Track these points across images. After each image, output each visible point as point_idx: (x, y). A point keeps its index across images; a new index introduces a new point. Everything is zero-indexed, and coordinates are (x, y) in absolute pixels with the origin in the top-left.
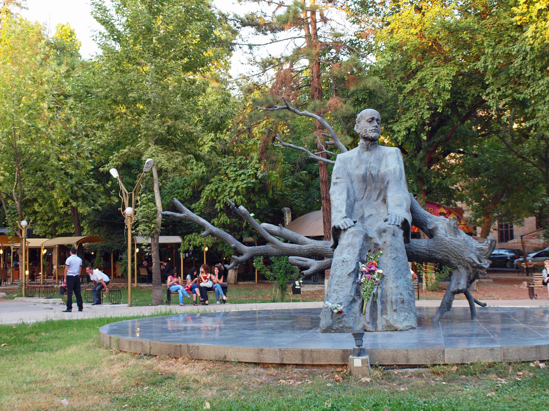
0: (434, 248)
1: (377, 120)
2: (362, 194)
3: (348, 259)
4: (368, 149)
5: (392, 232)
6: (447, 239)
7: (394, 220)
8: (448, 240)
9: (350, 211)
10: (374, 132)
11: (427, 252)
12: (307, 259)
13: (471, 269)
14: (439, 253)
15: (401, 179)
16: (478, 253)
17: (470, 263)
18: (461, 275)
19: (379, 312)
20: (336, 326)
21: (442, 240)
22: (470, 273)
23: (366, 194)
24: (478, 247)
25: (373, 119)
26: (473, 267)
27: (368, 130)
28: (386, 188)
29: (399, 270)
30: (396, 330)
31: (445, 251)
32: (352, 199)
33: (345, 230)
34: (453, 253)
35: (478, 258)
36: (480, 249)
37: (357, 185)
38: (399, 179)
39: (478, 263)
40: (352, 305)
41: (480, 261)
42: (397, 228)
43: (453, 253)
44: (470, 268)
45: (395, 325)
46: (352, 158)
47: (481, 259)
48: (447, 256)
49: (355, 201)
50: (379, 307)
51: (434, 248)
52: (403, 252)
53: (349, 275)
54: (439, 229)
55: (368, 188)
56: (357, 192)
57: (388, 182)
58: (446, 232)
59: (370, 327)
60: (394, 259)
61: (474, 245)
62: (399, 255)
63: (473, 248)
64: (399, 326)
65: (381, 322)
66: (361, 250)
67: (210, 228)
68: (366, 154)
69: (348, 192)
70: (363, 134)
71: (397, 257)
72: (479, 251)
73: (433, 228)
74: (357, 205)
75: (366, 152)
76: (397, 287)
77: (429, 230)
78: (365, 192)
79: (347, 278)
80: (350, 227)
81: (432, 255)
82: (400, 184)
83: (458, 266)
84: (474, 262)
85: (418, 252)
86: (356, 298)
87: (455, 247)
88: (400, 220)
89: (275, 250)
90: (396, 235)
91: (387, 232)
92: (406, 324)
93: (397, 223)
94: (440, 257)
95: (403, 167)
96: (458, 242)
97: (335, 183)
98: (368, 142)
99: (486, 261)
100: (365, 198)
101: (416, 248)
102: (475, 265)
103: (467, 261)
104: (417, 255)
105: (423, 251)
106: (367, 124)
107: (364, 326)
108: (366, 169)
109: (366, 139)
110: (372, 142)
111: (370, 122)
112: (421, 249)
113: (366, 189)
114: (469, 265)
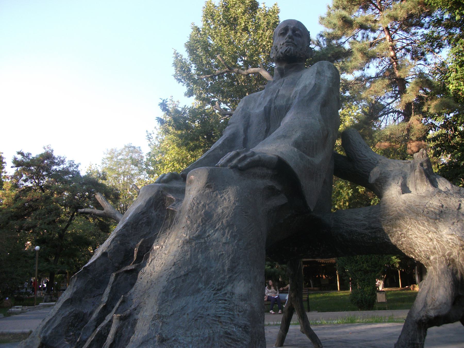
11: (367, 232)
38: (307, 98)
98: (283, 66)
108: (270, 101)
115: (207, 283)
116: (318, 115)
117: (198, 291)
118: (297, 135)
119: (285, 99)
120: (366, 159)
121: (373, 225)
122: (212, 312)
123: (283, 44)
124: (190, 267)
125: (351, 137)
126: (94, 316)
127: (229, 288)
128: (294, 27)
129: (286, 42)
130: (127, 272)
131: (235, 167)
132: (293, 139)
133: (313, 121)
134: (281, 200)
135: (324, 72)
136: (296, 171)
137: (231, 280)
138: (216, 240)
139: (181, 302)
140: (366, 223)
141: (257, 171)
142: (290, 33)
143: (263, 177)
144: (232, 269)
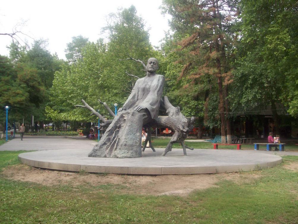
1: (154, 63)
6: (171, 117)
15: (156, 89)
17: (179, 129)
19: (114, 150)
20: (93, 154)
25: (151, 62)
29: (131, 131)
30: (118, 158)
32: (136, 99)
39: (181, 129)
40: (104, 146)
42: (137, 112)
45: (117, 156)
46: (142, 81)
49: (138, 100)
50: (115, 147)
55: (145, 94)
56: (139, 95)
59: (108, 156)
60: (129, 126)
64: (119, 156)
65: (113, 154)
72: (184, 123)
76: (125, 139)
78: (143, 96)
86: (107, 143)
88: (141, 108)
91: (130, 114)
92: (124, 155)
93: (137, 110)
95: (159, 85)
105: (163, 123)
107: (106, 155)
111: (150, 64)
113: (144, 94)
115: (132, 133)
116: (156, 95)
117: (131, 134)
118: (151, 102)
122: (133, 138)
126: (112, 138)
130: (117, 131)
131: (137, 111)
132: (150, 103)
134: (146, 117)
136: (150, 111)
137: (137, 133)
139: (129, 136)
141: (142, 111)
142: (152, 64)
144: (137, 131)
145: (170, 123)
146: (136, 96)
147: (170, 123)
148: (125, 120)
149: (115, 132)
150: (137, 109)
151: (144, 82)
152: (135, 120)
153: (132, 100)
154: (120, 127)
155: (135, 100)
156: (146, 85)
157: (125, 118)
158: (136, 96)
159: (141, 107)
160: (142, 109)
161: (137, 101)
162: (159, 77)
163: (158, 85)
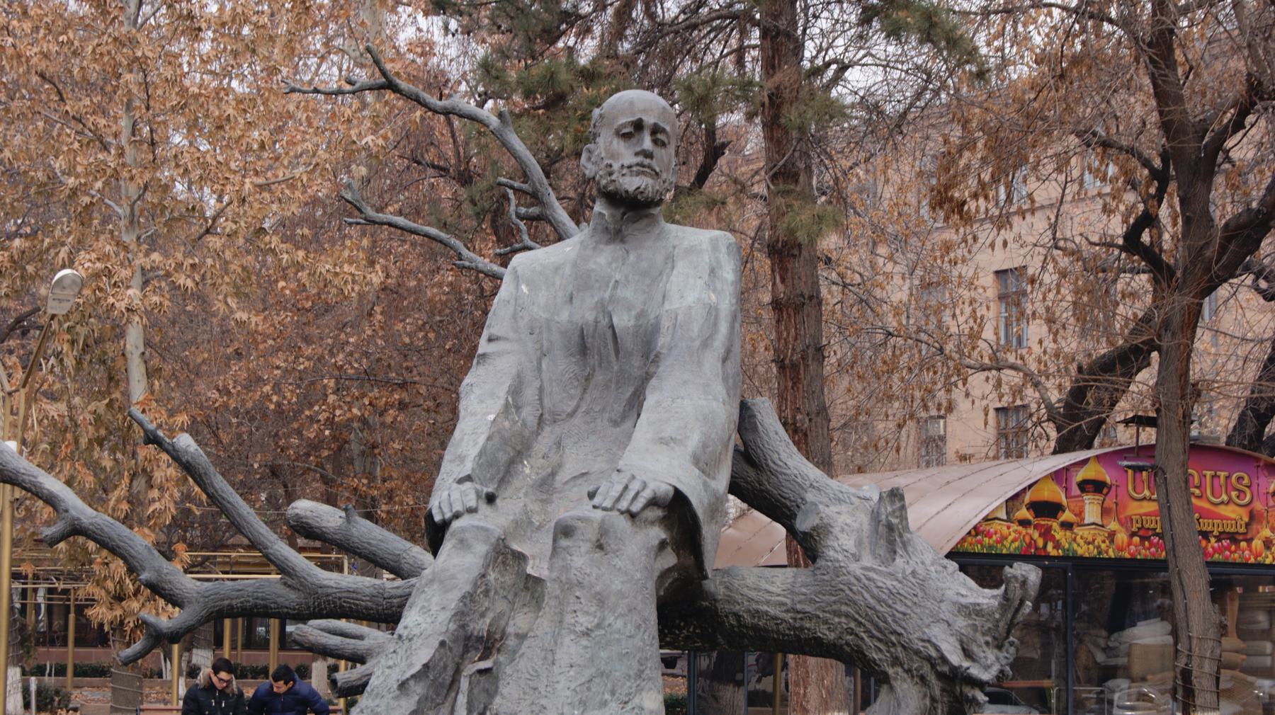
0: (812, 601)
1: (656, 130)
2: (572, 397)
3: (416, 631)
4: (616, 235)
5: (592, 534)
6: (854, 567)
7: (615, 493)
8: (859, 572)
9: (503, 457)
10: (638, 174)
11: (787, 616)
12: (362, 628)
13: (936, 686)
14: (826, 622)
15: (706, 344)
16: (961, 623)
17: (928, 659)
18: (899, 705)
21: (838, 571)
22: (933, 700)
23: (588, 397)
24: (963, 601)
25: (638, 125)
26: (941, 676)
27: (616, 166)
28: (647, 377)
31: (847, 616)
33: (445, 525)
34: (871, 621)
35: (961, 642)
36: (972, 611)
37: (561, 366)
38: (697, 343)
39: (956, 658)
41: (968, 654)
42: (623, 523)
43: (871, 621)
44: (932, 678)
46: (557, 269)
47: (975, 649)
48: (851, 632)
51: (812, 601)
52: (631, 610)
53: (403, 686)
54: (836, 531)
55: (599, 377)
57: (657, 356)
58: (859, 544)
60: (587, 633)
61: (950, 594)
62: (611, 619)
63: (943, 606)
66: (469, 598)
67: (73, 513)
68: (605, 258)
69: (516, 390)
70: (604, 182)
71: (598, 626)
73: (814, 529)
74: (544, 442)
75: (611, 247)
77: (805, 533)
78: (585, 390)
79: (396, 698)
80: (457, 516)
81: (802, 629)
82: (700, 363)
83: (891, 671)
84: (944, 659)
85: (757, 614)
87: (879, 601)
88: (647, 495)
89: (293, 596)
90: (611, 543)
93: (624, 505)
94: (832, 636)
96: (889, 583)
97: (484, 355)
99: (990, 655)
100: (579, 414)
101: (751, 600)
102: (946, 669)
103: (917, 652)
104: (756, 628)
105: (773, 611)
106: (618, 145)
109: (615, 198)
110: (633, 210)
111: (626, 136)
112: (768, 603)
113: (587, 379)
114: (926, 669)
115: (613, 693)
117: (604, 704)
118: (694, 440)
119: (634, 313)
120: (788, 472)
121: (799, 607)
123: (630, 167)
124: (593, 670)
125: (759, 417)
127: (636, 701)
128: (655, 124)
129: (637, 165)
130: (480, 672)
132: (690, 449)
133: (714, 404)
134: (670, 559)
135: (721, 267)
137: (640, 690)
138: (619, 631)
140: (788, 601)
143: (652, 523)
144: (639, 674)
145: (837, 614)
146: (530, 394)
147: (837, 614)
148: (538, 581)
149: (464, 684)
150: (618, 500)
151: (583, 281)
152: (617, 585)
153: (507, 424)
154: (488, 644)
155: (524, 424)
156: (604, 309)
157: (529, 570)
158: (530, 394)
159: (645, 486)
160: (653, 502)
161: (538, 434)
162: (714, 243)
163: (712, 311)
